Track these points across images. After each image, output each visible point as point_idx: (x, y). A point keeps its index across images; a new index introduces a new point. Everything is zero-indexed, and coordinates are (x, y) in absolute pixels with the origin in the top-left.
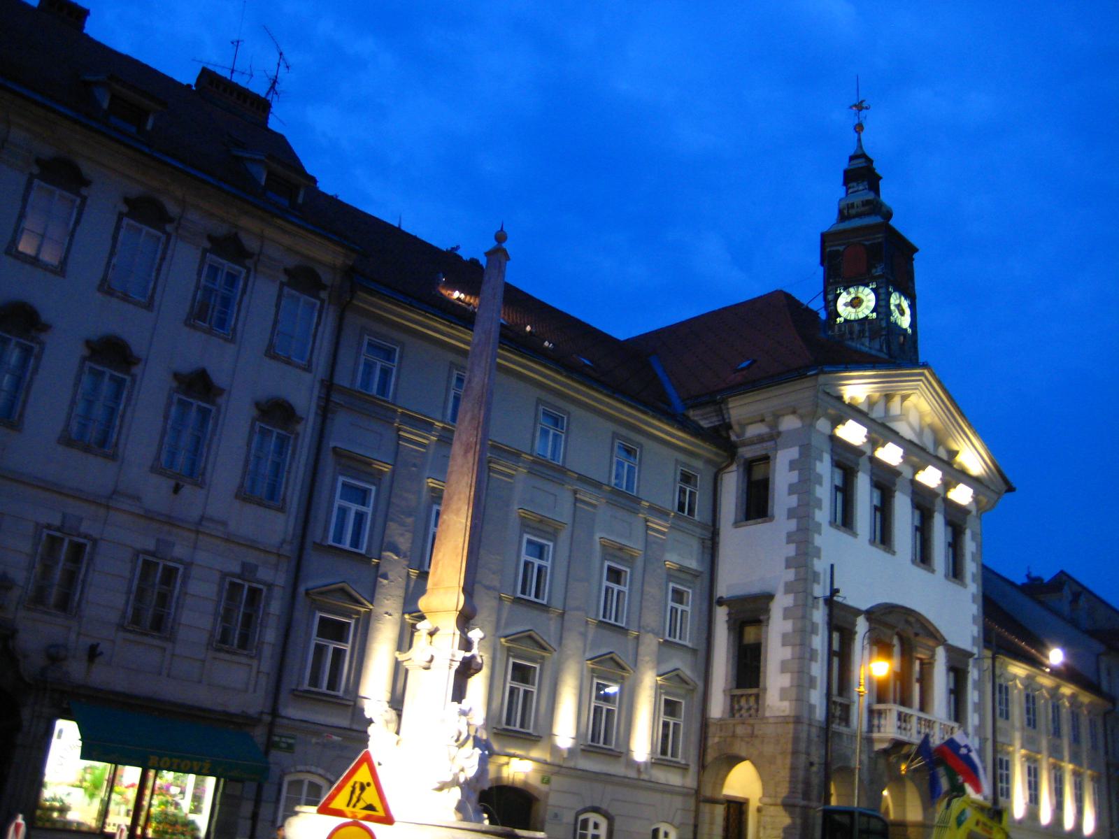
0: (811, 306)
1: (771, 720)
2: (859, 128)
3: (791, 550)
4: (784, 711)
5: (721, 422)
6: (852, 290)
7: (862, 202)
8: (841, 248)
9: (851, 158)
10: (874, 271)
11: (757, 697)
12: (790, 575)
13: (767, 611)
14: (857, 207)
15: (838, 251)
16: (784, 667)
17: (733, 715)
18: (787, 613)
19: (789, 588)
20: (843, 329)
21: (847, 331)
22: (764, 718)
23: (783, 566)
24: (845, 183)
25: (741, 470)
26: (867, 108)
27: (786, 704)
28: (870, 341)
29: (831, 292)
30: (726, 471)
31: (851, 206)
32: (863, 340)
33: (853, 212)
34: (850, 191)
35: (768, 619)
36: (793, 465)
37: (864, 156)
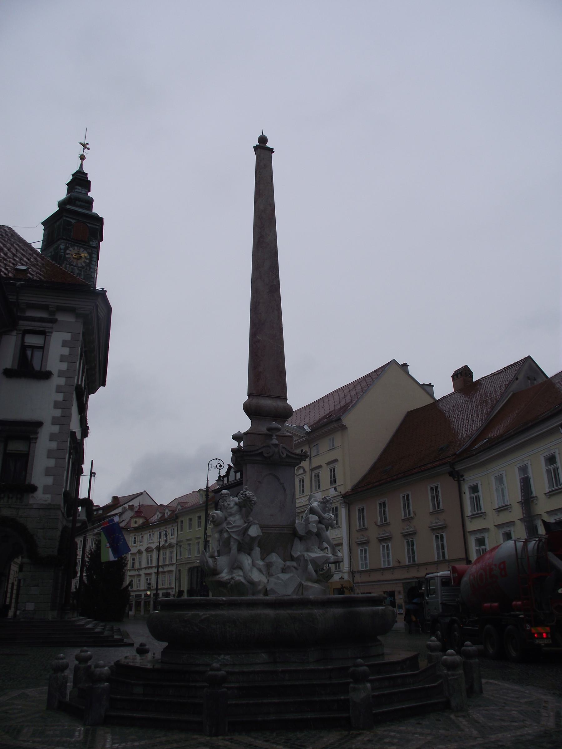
0: (33, 245)
1: (35, 507)
2: (82, 158)
3: (60, 397)
4: (46, 501)
5: (15, 300)
6: (76, 248)
8: (73, 221)
9: (77, 172)
10: (91, 243)
12: (58, 413)
13: (37, 433)
15: (71, 222)
18: (53, 437)
20: (68, 268)
23: (52, 405)
24: (71, 185)
25: (20, 335)
27: (48, 497)
34: (76, 190)
35: (37, 438)
36: (65, 344)
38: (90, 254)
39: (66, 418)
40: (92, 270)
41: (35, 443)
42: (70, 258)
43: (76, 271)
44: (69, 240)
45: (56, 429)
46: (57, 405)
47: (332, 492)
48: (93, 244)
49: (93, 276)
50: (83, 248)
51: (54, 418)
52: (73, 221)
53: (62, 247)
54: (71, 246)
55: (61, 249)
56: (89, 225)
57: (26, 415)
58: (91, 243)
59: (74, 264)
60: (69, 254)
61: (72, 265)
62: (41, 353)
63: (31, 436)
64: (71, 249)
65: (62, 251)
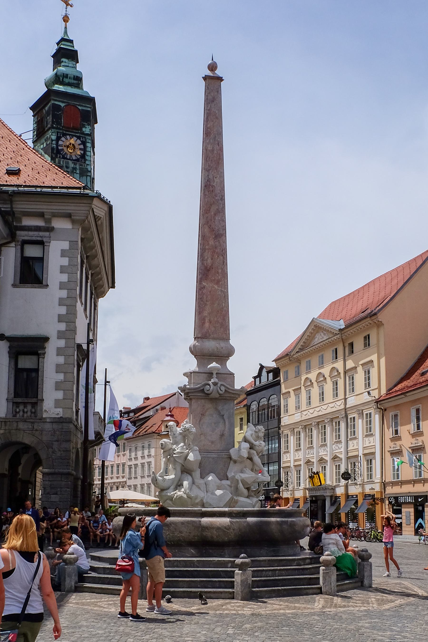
2: (66, 19)
6: (68, 137)
7: (74, 76)
8: (62, 105)
9: (63, 40)
10: (84, 129)
11: (34, 405)
12: (63, 327)
13: (45, 348)
14: (70, 78)
16: (58, 386)
17: (15, 416)
18: (59, 352)
19: (61, 335)
20: (62, 163)
21: (64, 165)
22: (41, 419)
23: (56, 319)
26: (71, 6)
28: (80, 177)
29: (54, 134)
30: (8, 245)
31: (66, 76)
32: (75, 174)
33: (66, 80)
34: (62, 64)
37: (71, 41)
38: (84, 143)
39: (72, 330)
40: (87, 162)
41: (44, 358)
42: (63, 149)
43: (71, 165)
44: (60, 129)
45: (62, 343)
46: (60, 319)
47: (366, 398)
48: (87, 130)
49: (88, 167)
50: (76, 136)
51: (59, 332)
52: (62, 105)
53: (54, 137)
54: (63, 136)
55: (52, 140)
56: (80, 108)
57: (32, 331)
58: (84, 129)
59: (68, 157)
60: (61, 145)
61: (66, 158)
62: (42, 264)
63: (39, 352)
64: (63, 139)
65: (54, 142)
